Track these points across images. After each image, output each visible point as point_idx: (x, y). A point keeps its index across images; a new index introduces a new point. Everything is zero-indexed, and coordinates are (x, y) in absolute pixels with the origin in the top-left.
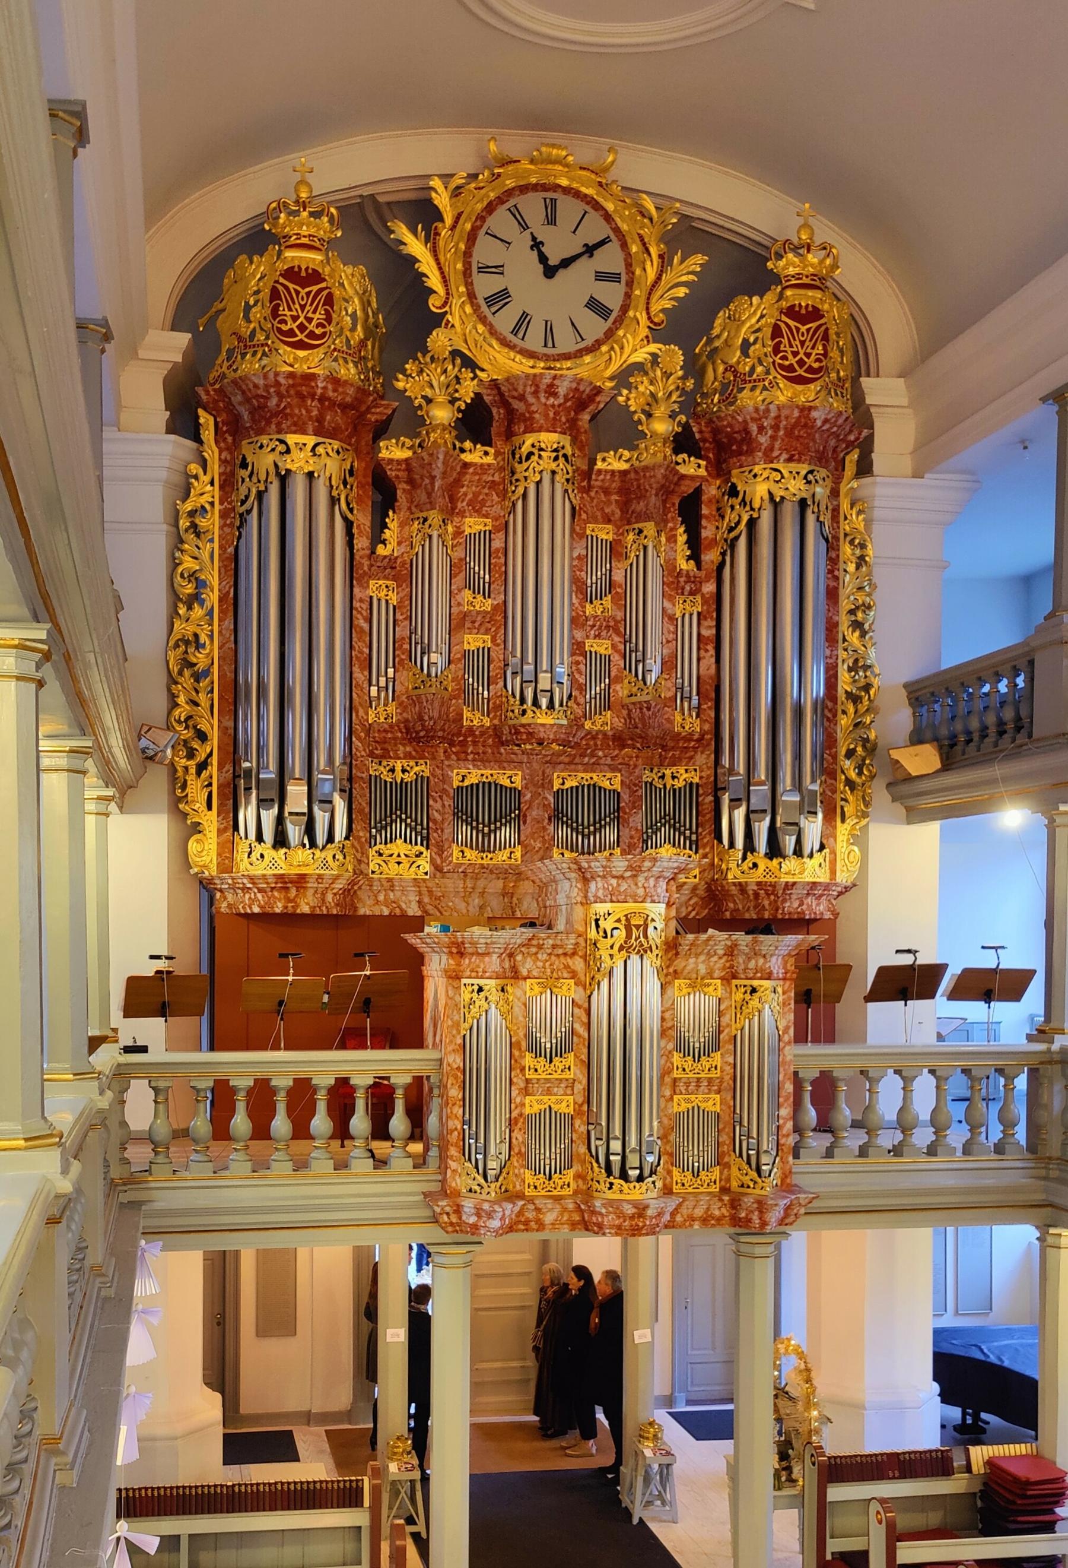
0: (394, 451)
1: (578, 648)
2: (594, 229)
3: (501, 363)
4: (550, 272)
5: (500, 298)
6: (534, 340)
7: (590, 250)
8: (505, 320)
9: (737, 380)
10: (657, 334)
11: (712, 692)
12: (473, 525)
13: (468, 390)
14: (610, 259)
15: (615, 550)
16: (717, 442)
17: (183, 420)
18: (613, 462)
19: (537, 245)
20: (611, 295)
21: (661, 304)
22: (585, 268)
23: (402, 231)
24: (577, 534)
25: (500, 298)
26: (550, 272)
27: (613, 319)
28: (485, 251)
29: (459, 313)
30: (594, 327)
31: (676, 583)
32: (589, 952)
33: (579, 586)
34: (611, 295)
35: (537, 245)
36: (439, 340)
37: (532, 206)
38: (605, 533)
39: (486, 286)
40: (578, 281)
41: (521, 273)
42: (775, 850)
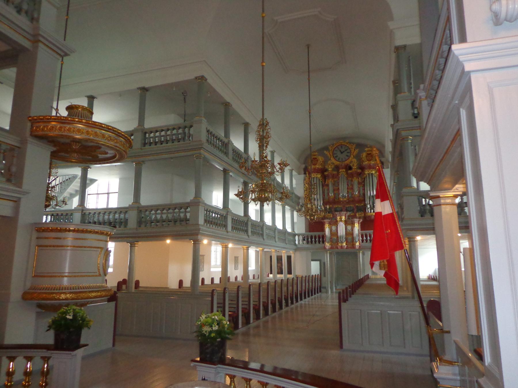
0: (326, 173)
1: (348, 192)
2: (346, 148)
3: (337, 163)
4: (342, 153)
5: (337, 156)
6: (340, 160)
7: (346, 150)
8: (337, 159)
9: (363, 161)
10: (354, 157)
11: (364, 195)
12: (335, 180)
13: (333, 166)
14: (348, 151)
15: (352, 181)
16: (362, 168)
17: (305, 173)
18: (350, 171)
19: (340, 151)
20: (349, 154)
21: (354, 154)
22: (346, 152)
23: (325, 152)
24: (347, 179)
25: (337, 156)
26: (342, 153)
27: (349, 157)
28: (335, 152)
29: (332, 159)
30: (347, 158)
31: (359, 183)
32: (337, 221)
33: (348, 185)
34: (349, 154)
35: (340, 151)
36: (329, 162)
37: (340, 147)
38: (350, 179)
39: (335, 155)
40: (345, 153)
41: (339, 153)
42: (371, 212)
